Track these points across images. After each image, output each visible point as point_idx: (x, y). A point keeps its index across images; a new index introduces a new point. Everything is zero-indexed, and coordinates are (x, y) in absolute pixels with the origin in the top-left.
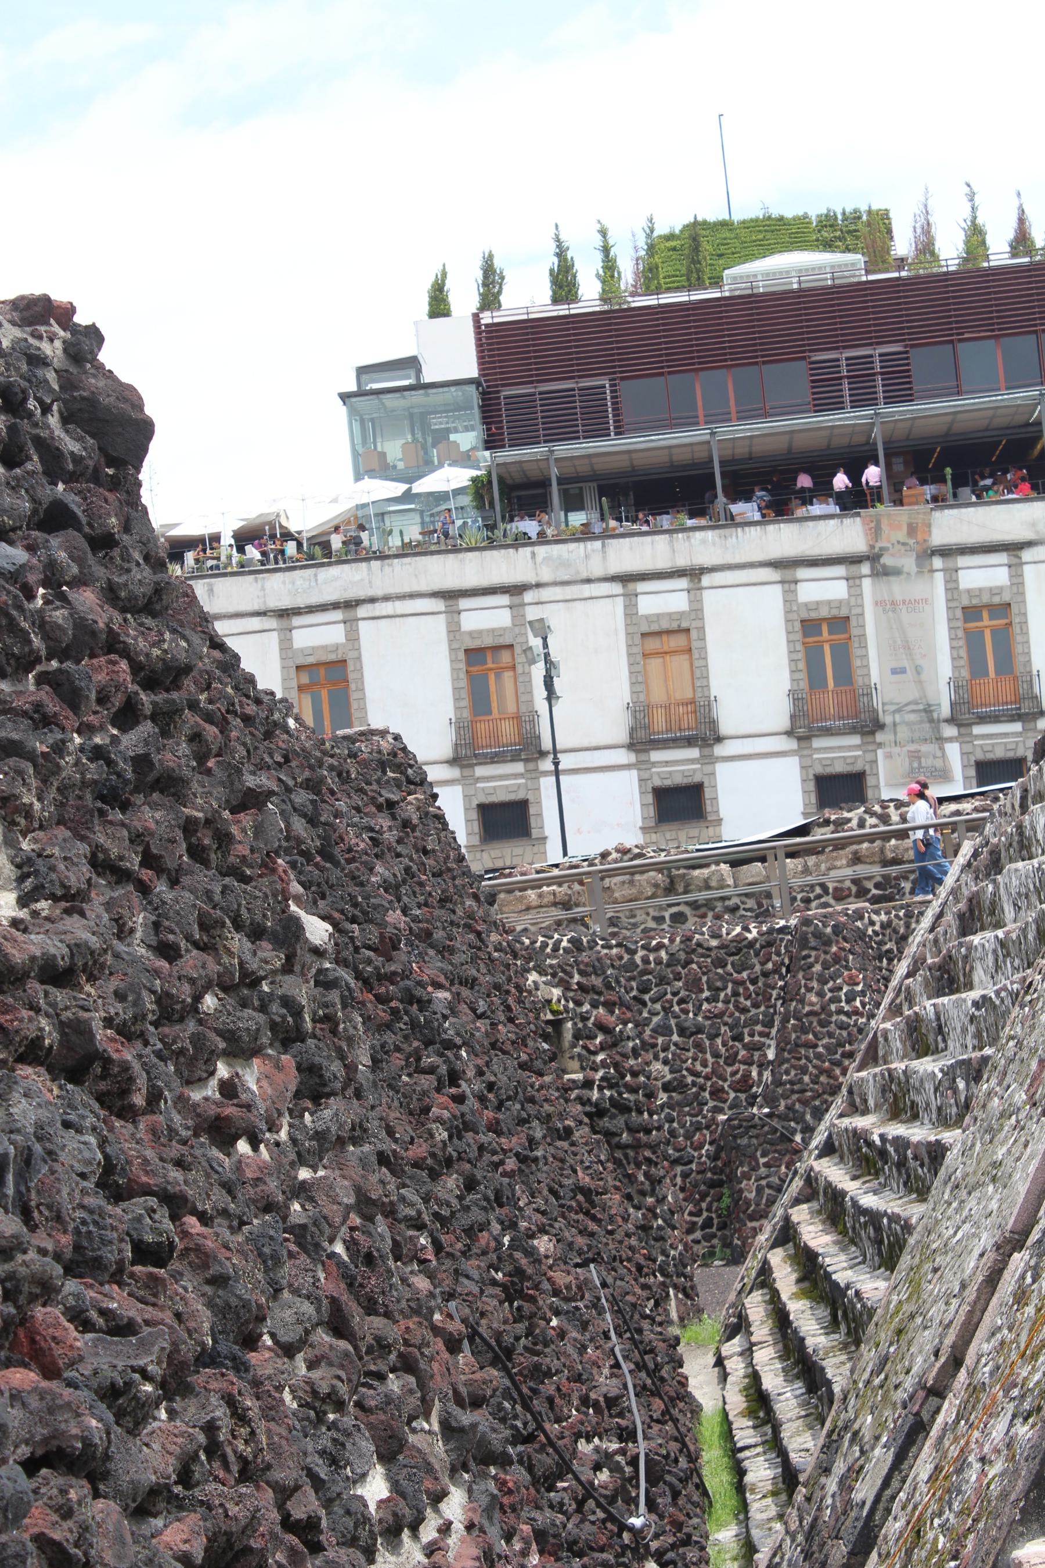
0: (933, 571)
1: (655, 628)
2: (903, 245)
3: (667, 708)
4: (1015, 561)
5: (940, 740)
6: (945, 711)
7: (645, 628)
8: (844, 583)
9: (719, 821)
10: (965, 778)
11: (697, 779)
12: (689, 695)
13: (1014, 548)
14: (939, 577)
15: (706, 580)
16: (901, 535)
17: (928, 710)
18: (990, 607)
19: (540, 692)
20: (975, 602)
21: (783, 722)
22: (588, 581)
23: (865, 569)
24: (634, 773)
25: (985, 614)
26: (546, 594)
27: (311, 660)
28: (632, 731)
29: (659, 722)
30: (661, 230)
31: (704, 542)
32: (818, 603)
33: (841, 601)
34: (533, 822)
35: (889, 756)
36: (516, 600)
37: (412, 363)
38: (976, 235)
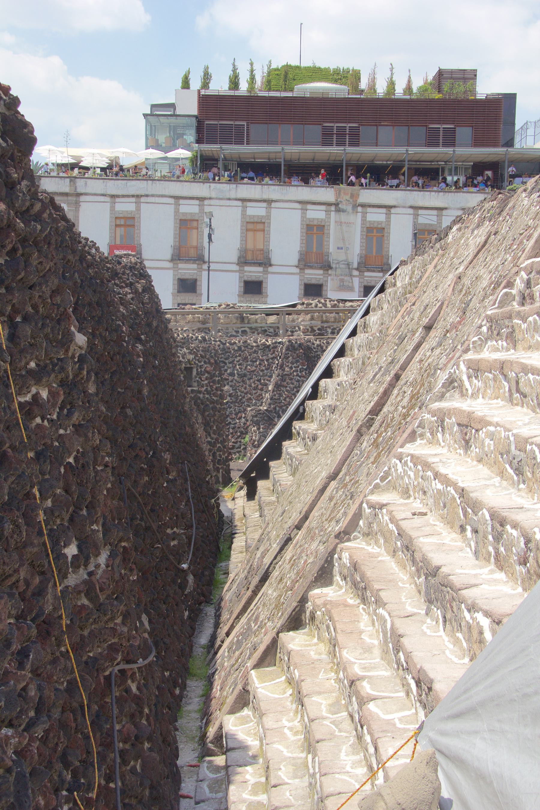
0: (357, 212)
1: (252, 220)
2: (364, 84)
3: (253, 251)
5: (351, 276)
6: (355, 265)
7: (248, 220)
9: (267, 296)
10: (359, 291)
11: (261, 279)
13: (389, 207)
14: (359, 215)
15: (273, 205)
16: (348, 197)
18: (377, 228)
19: (206, 239)
20: (372, 226)
21: (296, 263)
22: (229, 199)
23: (333, 208)
24: (238, 274)
25: (375, 231)
26: (212, 202)
27: (121, 215)
28: (239, 258)
30: (274, 66)
31: (274, 190)
35: (332, 280)
36: (201, 203)
37: (172, 106)
38: (392, 84)
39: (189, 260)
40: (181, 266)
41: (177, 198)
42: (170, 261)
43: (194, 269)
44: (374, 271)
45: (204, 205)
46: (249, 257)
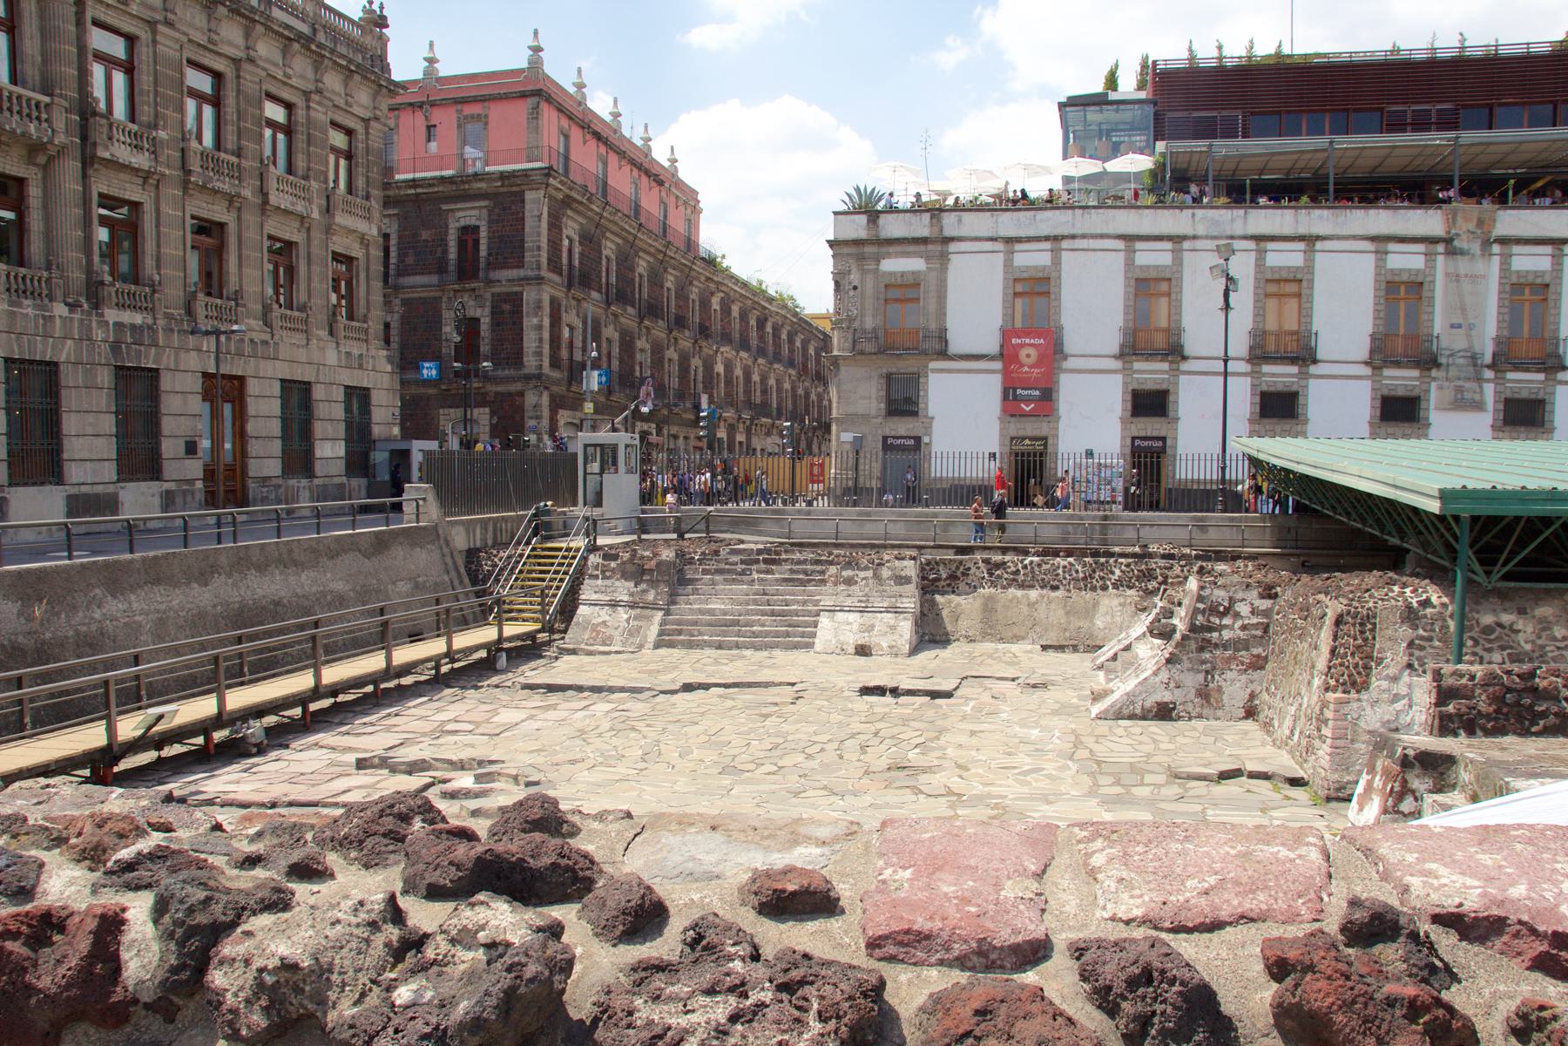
0: (1491, 255)
1: (1276, 276)
4: (1557, 252)
6: (1488, 359)
7: (1269, 276)
8: (1422, 257)
9: (1306, 421)
10: (1495, 410)
11: (1294, 388)
12: (1296, 328)
14: (1496, 260)
15: (1319, 245)
16: (1471, 226)
17: (1474, 358)
18: (1532, 285)
23: (1440, 248)
24: (1249, 379)
25: (1527, 291)
26: (1199, 244)
27: (1025, 275)
29: (1271, 347)
31: (1320, 217)
32: (1401, 270)
33: (1418, 270)
34: (1171, 407)
35: (1440, 388)
36: (1177, 246)
39: (1152, 355)
40: (1137, 365)
41: (1129, 239)
42: (1115, 357)
43: (1163, 372)
44: (1527, 370)
45: (1182, 250)
46: (1271, 347)
